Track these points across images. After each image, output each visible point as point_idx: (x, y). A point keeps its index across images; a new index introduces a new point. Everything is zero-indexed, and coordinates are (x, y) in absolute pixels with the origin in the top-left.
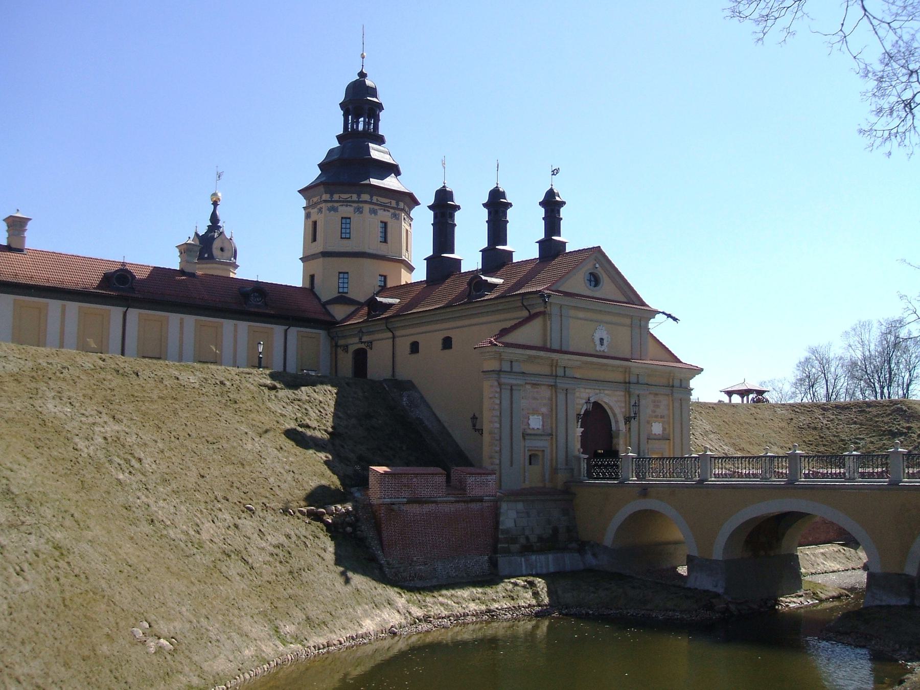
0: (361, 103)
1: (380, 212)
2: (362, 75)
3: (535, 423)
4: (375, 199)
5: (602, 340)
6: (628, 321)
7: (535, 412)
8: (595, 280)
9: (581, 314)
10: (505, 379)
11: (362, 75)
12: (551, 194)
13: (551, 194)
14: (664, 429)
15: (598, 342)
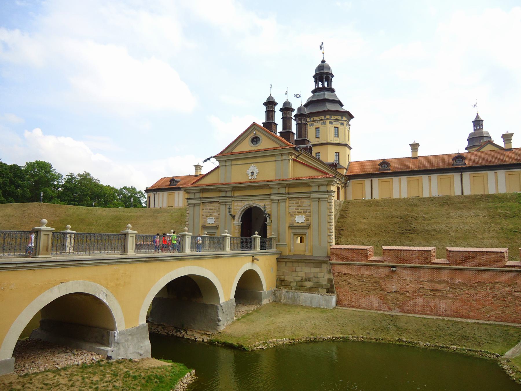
0: (323, 75)
1: (335, 123)
2: (323, 61)
3: (211, 221)
4: (312, 119)
5: (252, 173)
6: (273, 159)
7: (211, 215)
8: (255, 140)
9: (240, 162)
10: (191, 202)
11: (323, 61)
12: (270, 98)
13: (270, 98)
14: (307, 220)
15: (250, 175)
